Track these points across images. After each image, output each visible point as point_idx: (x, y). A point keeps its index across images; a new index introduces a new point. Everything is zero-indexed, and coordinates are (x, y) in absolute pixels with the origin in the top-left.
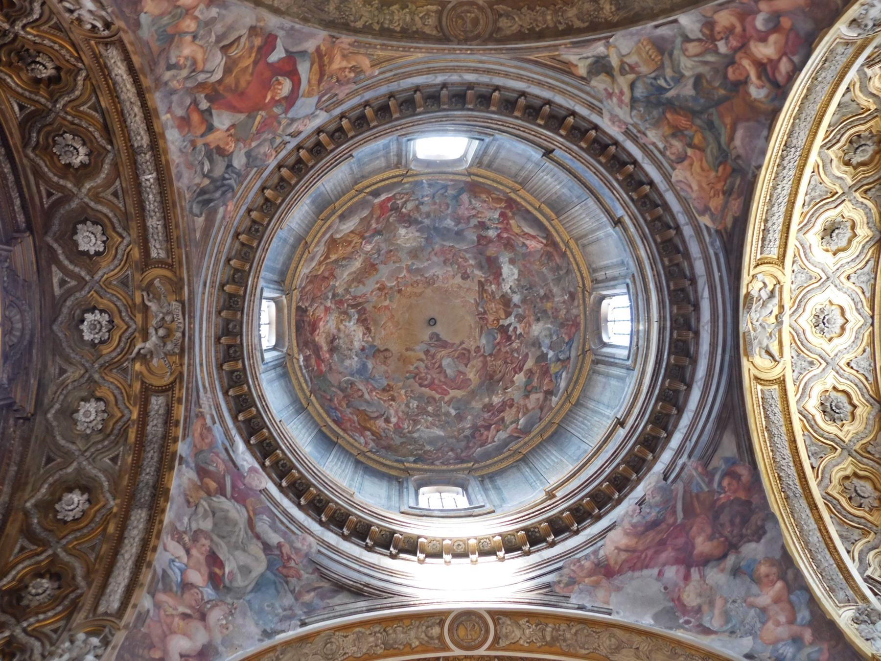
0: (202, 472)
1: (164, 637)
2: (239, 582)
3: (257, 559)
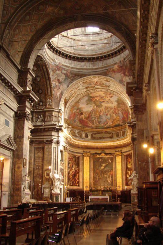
0: (53, 71)
1: (56, 95)
2: (62, 81)
3: (64, 76)
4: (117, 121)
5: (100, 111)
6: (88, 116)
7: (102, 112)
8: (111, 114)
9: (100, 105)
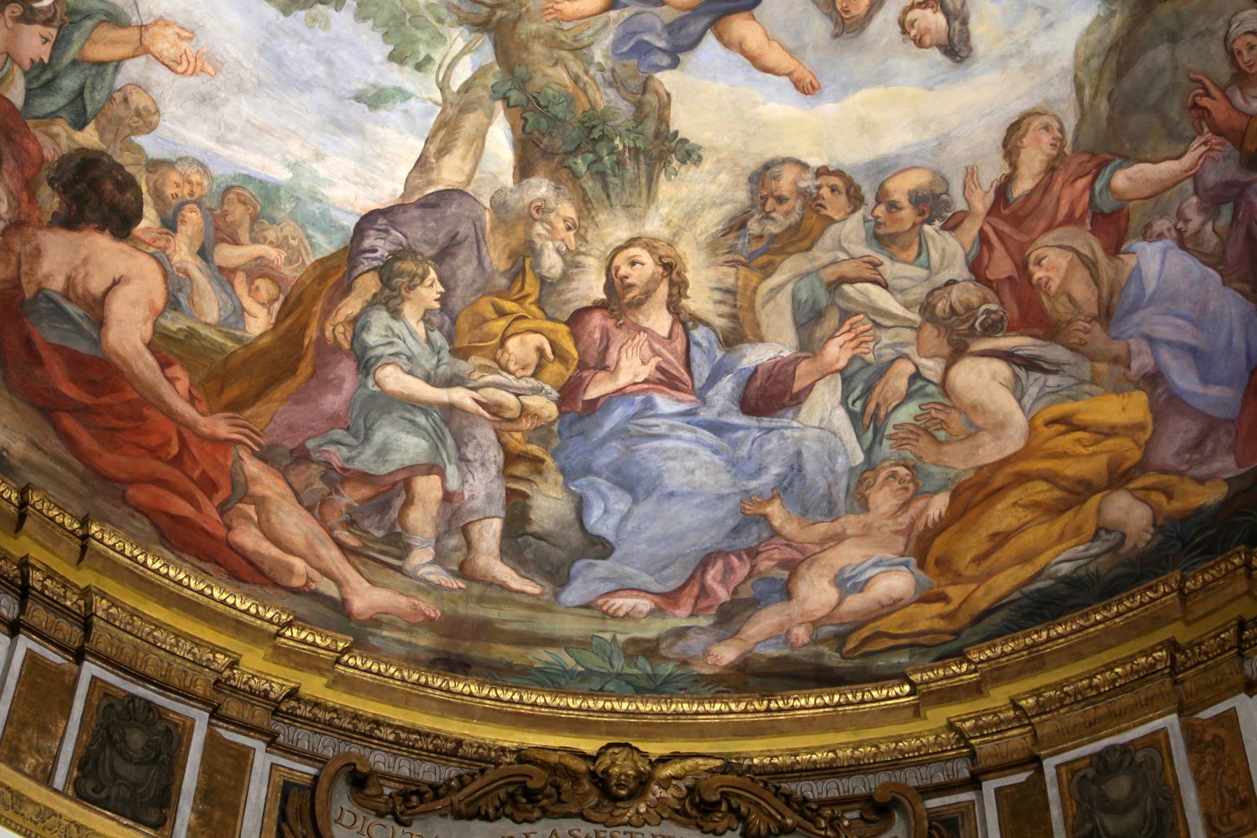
4: (1081, 491)
5: (591, 286)
6: (258, 323)
7: (659, 320)
8: (883, 370)
9: (605, 98)
